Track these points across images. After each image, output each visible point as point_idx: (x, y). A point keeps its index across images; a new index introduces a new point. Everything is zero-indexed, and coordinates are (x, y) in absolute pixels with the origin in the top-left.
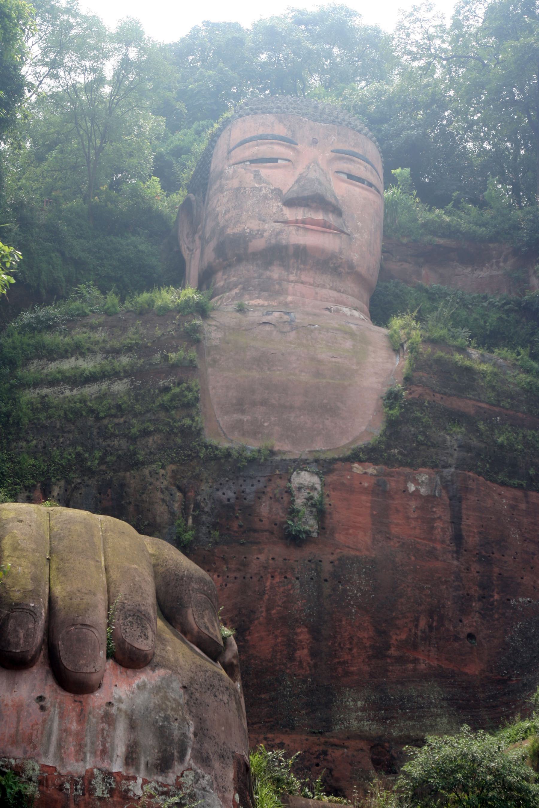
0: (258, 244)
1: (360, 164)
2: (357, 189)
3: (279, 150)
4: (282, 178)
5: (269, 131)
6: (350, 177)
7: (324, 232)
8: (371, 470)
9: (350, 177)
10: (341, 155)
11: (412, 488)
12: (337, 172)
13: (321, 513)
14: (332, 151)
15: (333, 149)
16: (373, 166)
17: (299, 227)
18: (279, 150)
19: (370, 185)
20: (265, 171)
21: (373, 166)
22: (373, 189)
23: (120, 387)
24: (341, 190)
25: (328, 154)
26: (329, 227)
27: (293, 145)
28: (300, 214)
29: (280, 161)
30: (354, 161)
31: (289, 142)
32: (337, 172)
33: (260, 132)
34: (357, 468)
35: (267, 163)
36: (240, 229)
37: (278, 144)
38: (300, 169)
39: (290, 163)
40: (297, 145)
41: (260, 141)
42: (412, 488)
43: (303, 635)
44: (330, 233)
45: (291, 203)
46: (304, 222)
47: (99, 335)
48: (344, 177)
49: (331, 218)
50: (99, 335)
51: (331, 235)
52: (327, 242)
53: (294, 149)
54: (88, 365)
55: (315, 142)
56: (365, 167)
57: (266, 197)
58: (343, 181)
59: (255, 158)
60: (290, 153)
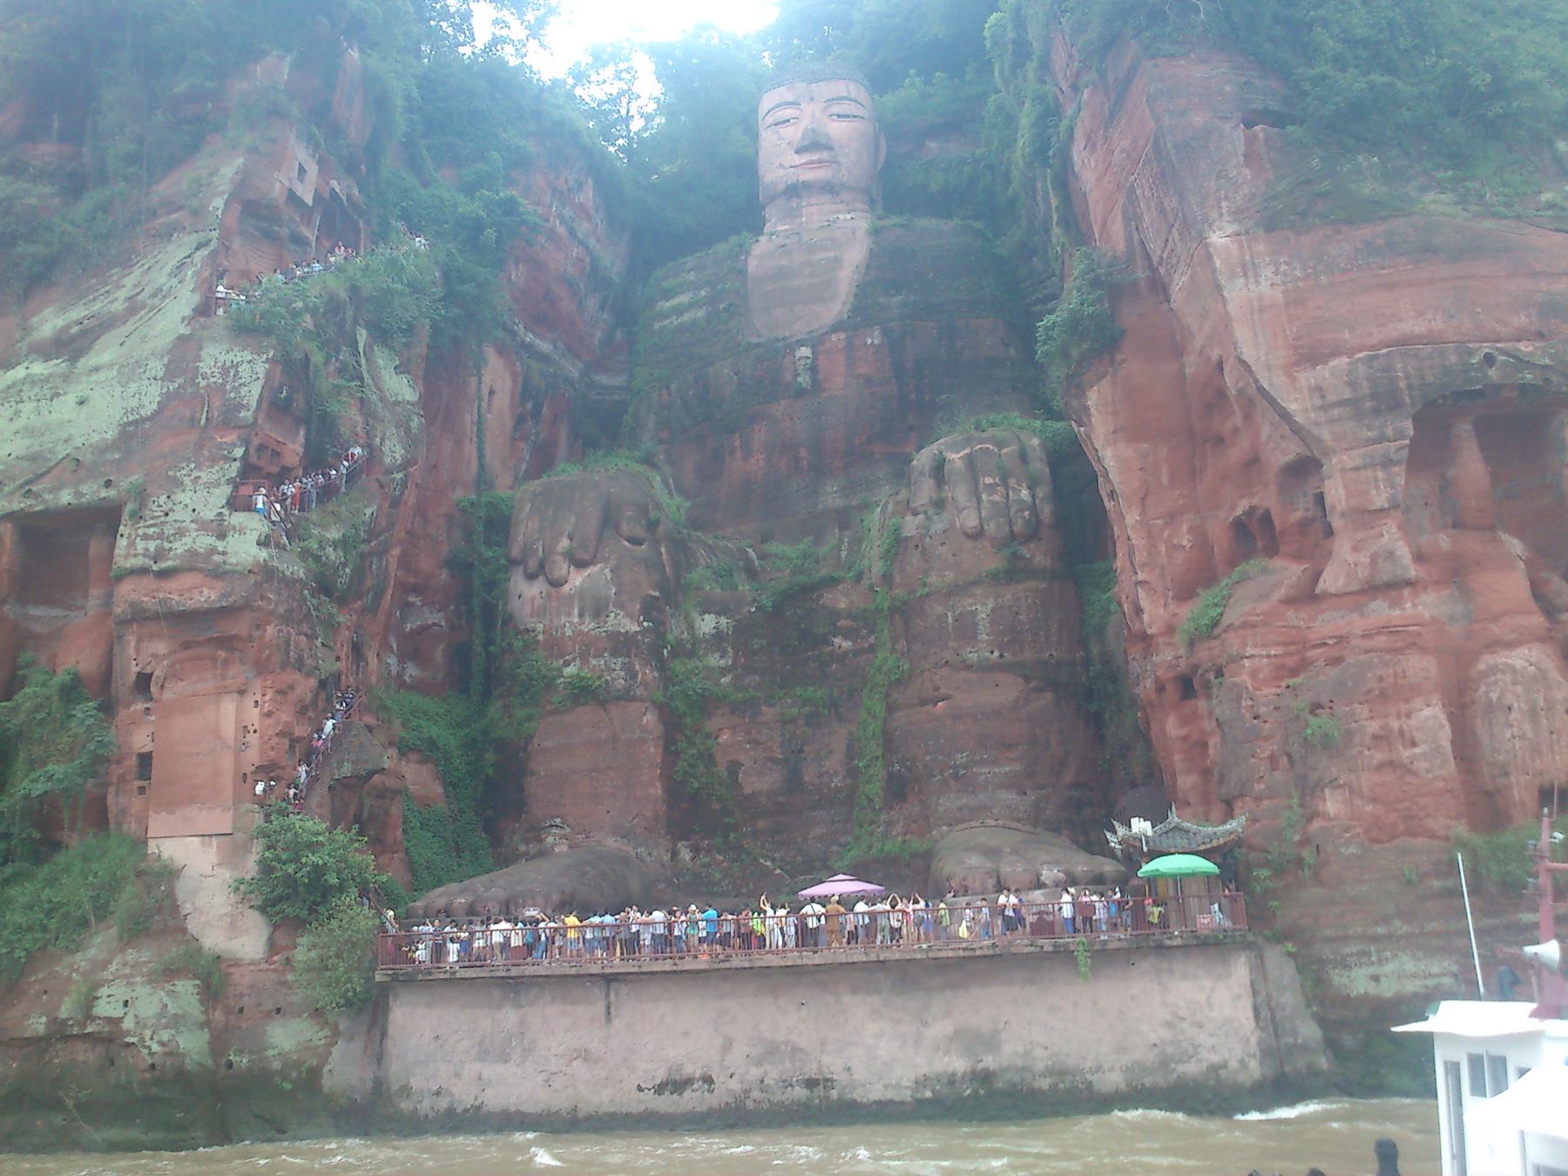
0: (782, 187)
3: (789, 112)
4: (794, 133)
8: (842, 336)
10: (830, 101)
11: (869, 341)
13: (813, 370)
18: (789, 112)
20: (783, 131)
23: (701, 313)
28: (806, 158)
31: (795, 104)
34: (834, 337)
42: (869, 341)
43: (803, 453)
45: (798, 152)
47: (692, 277)
49: (825, 155)
50: (692, 277)
54: (684, 299)
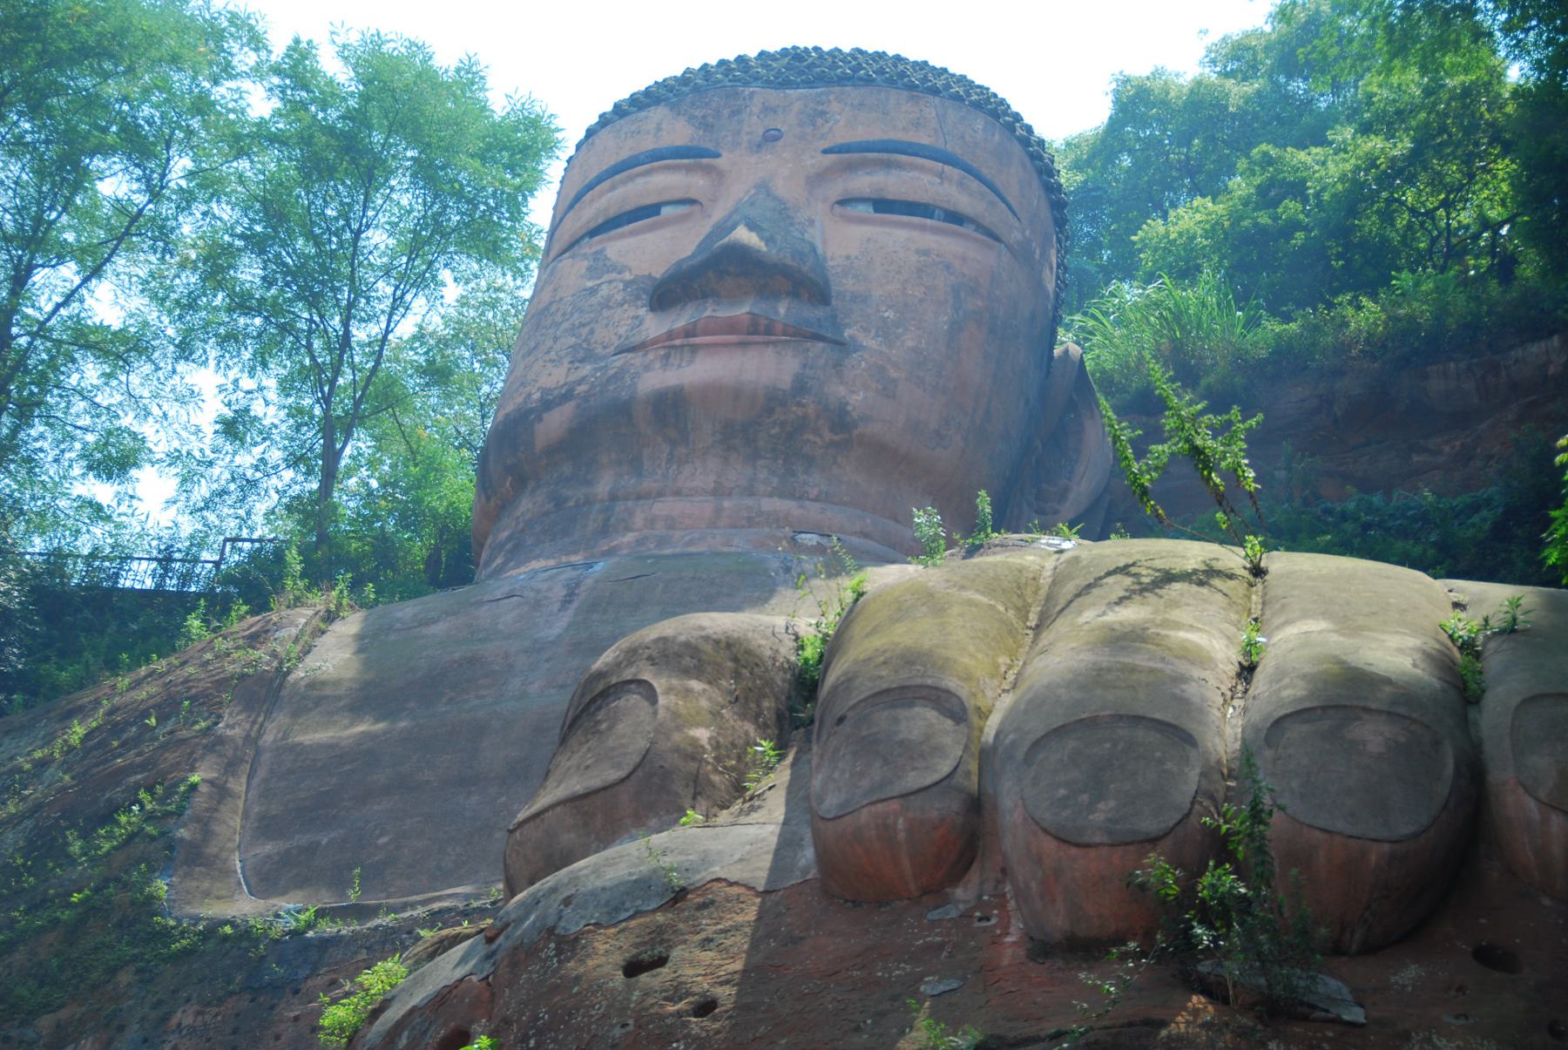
0: (555, 423)
1: (922, 169)
2: (902, 234)
5: (648, 144)
6: (883, 205)
7: (743, 345)
9: (883, 205)
12: (842, 202)
14: (825, 152)
15: (826, 145)
16: (968, 169)
17: (674, 347)
19: (955, 218)
21: (968, 169)
22: (967, 230)
24: (845, 243)
25: (815, 161)
26: (769, 331)
27: (705, 161)
28: (680, 319)
29: (666, 211)
30: (899, 166)
32: (842, 202)
33: (625, 154)
35: (629, 222)
36: (520, 400)
37: (668, 168)
38: (718, 213)
39: (696, 208)
40: (718, 156)
41: (617, 177)
44: (767, 343)
46: (689, 332)
48: (865, 210)
51: (770, 350)
52: (765, 368)
53: (708, 170)
55: (771, 138)
56: (941, 175)
57: (606, 304)
58: (862, 221)
59: (600, 221)
60: (696, 184)
